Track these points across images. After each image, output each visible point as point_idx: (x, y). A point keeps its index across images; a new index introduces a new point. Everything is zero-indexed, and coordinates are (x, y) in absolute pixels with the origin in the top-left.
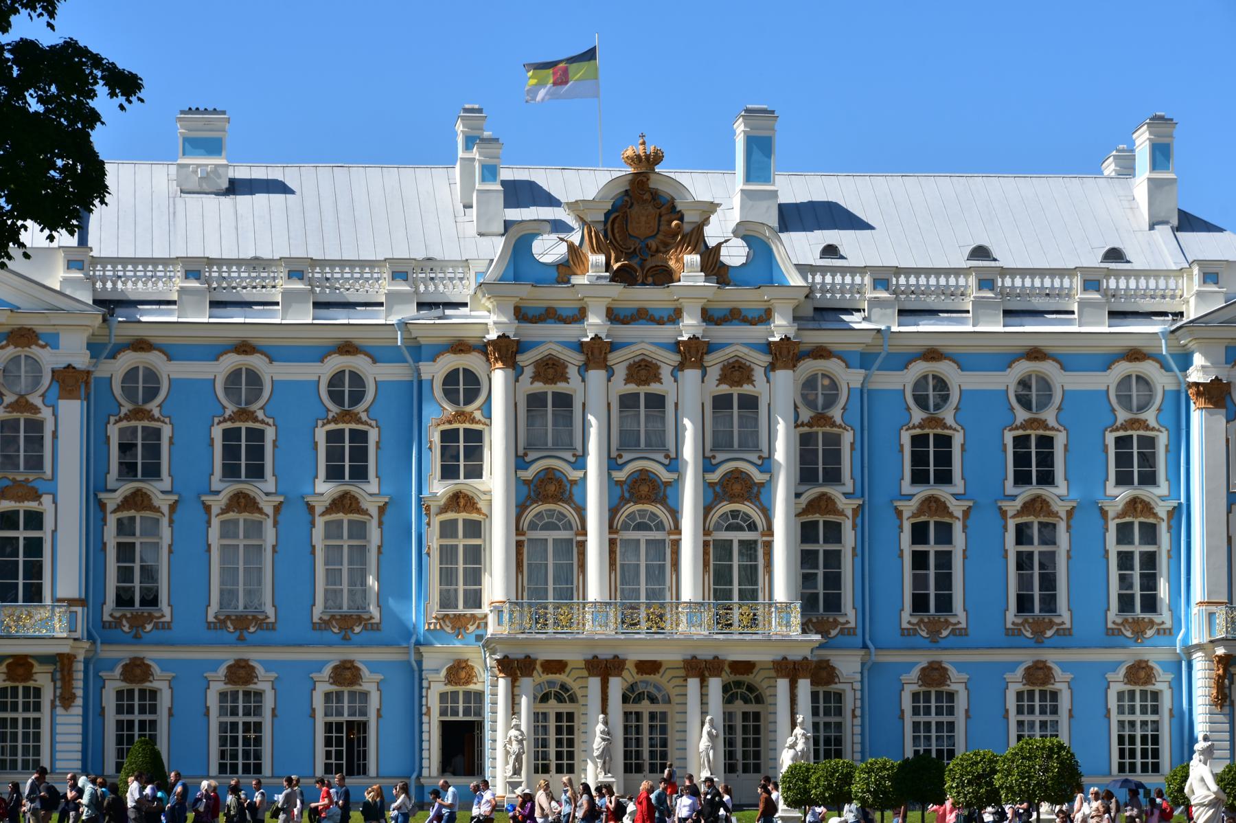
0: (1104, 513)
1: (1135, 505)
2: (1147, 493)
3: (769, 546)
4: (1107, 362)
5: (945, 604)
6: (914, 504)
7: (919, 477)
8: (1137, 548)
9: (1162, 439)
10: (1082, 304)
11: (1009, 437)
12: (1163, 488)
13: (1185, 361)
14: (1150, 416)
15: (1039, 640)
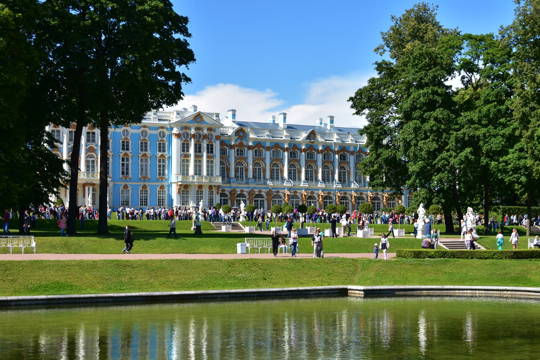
0: (156, 157)
1: (162, 156)
2: (164, 153)
3: (97, 161)
4: (157, 129)
5: (127, 173)
6: (123, 154)
7: (123, 149)
8: (162, 164)
9: (167, 143)
10: (153, 118)
11: (140, 142)
12: (167, 153)
13: (172, 129)
14: (165, 139)
15: (145, 181)
